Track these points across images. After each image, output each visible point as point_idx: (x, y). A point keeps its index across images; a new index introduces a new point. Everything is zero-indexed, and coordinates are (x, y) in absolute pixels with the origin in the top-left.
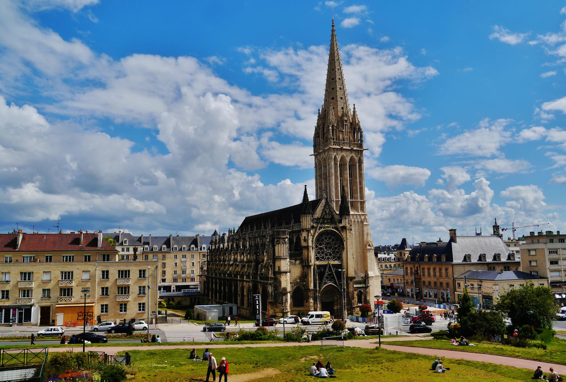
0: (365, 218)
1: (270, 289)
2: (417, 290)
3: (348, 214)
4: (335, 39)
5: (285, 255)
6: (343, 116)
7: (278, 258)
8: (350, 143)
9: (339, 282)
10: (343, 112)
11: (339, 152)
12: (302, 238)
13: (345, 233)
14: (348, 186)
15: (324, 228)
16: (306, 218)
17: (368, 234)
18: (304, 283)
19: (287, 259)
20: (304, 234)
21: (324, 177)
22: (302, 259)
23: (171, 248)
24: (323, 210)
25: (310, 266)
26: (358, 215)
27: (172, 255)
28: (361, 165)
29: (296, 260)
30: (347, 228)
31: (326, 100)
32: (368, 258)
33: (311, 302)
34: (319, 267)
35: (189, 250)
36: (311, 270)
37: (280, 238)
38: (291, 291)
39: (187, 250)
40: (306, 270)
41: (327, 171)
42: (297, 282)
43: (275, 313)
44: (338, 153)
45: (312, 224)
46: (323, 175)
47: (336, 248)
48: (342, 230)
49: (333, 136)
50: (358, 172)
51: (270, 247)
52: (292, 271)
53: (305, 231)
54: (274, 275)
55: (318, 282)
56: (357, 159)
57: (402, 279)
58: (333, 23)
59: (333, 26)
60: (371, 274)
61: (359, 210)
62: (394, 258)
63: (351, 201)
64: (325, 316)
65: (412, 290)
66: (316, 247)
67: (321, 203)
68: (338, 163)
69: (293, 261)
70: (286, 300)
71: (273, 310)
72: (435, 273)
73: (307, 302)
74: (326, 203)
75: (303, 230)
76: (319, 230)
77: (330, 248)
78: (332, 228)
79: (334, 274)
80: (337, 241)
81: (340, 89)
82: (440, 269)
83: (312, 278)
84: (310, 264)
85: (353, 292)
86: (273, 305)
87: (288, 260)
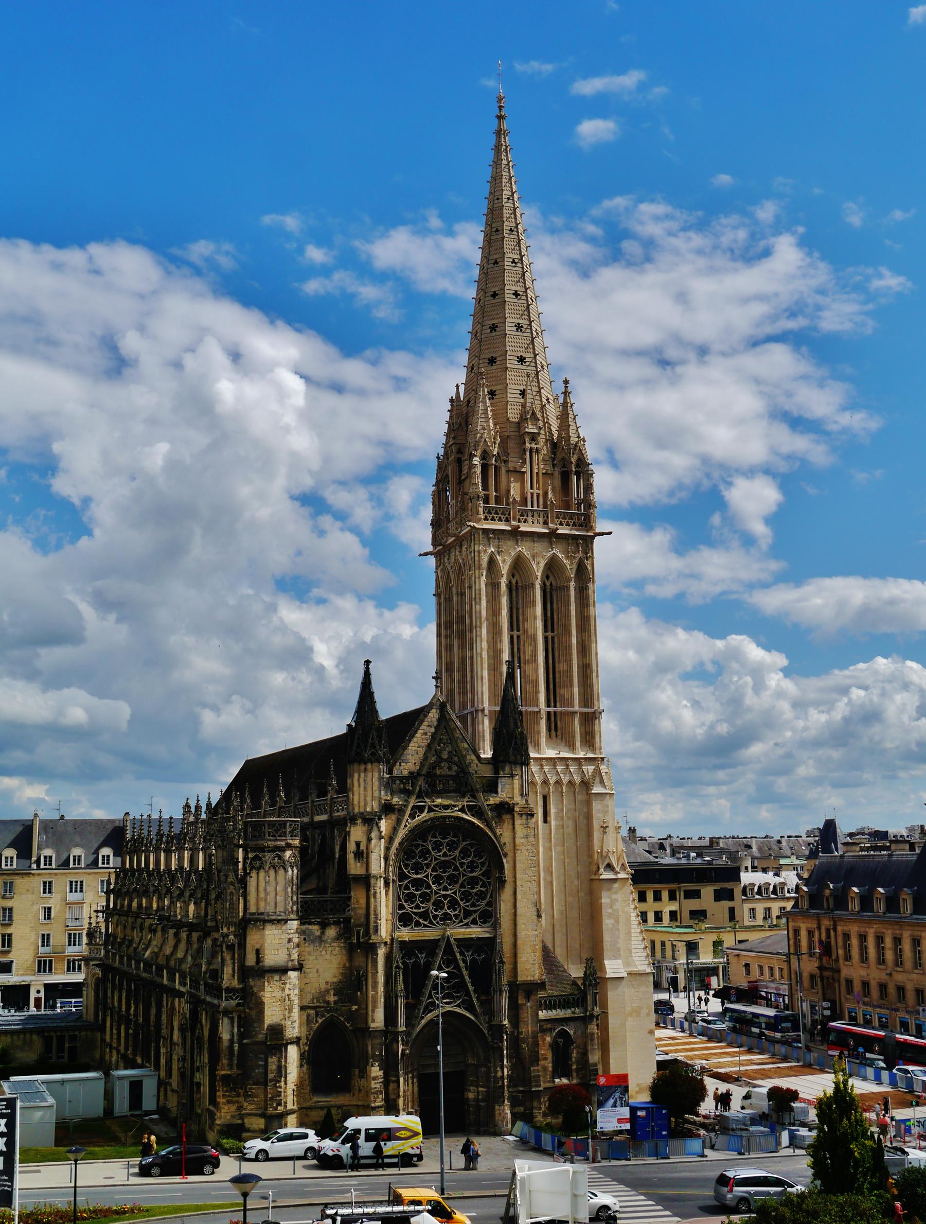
0: (598, 772)
2: (825, 1009)
3: (525, 761)
4: (505, 162)
5: (280, 908)
6: (523, 419)
7: (257, 920)
8: (546, 513)
9: (482, 1003)
10: (524, 406)
11: (508, 545)
12: (351, 847)
13: (507, 826)
14: (536, 661)
15: (430, 810)
16: (362, 775)
17: (604, 828)
18: (354, 1008)
19: (286, 921)
20: (357, 833)
21: (458, 631)
22: (347, 921)
23: (34, 859)
24: (429, 746)
25: (372, 949)
26: (570, 762)
27: (36, 883)
28: (587, 588)
29: (324, 926)
30: (517, 809)
31: (472, 368)
32: (606, 911)
33: (373, 1075)
34: (408, 948)
35: (94, 864)
36: (375, 962)
37: (262, 849)
38: (303, 1035)
39: (88, 866)
40: (359, 960)
41: (467, 607)
42: (328, 1002)
43: (242, 1117)
44: (504, 548)
45: (385, 796)
46: (458, 623)
47: (473, 882)
48: (499, 817)
49: (485, 486)
50: (573, 613)
51: (229, 880)
52: (308, 965)
53: (359, 821)
54: (240, 981)
55: (401, 1002)
56: (570, 566)
57: (785, 966)
58: (500, 108)
59: (500, 118)
60: (613, 967)
61: (578, 744)
62: (797, 886)
63: (549, 713)
64: (402, 1134)
65: (813, 1007)
66: (402, 876)
67: (426, 723)
68: (504, 581)
69: (315, 929)
70: (281, 1071)
71: (233, 1108)
72: (881, 951)
73: (361, 1077)
74: (439, 720)
75: (353, 819)
76: (412, 816)
77: (453, 880)
78: (462, 810)
80: (478, 855)
81: (519, 327)
82: (897, 940)
83: (381, 988)
84: (374, 939)
85: (535, 1037)
86: (233, 1089)
87: (294, 924)
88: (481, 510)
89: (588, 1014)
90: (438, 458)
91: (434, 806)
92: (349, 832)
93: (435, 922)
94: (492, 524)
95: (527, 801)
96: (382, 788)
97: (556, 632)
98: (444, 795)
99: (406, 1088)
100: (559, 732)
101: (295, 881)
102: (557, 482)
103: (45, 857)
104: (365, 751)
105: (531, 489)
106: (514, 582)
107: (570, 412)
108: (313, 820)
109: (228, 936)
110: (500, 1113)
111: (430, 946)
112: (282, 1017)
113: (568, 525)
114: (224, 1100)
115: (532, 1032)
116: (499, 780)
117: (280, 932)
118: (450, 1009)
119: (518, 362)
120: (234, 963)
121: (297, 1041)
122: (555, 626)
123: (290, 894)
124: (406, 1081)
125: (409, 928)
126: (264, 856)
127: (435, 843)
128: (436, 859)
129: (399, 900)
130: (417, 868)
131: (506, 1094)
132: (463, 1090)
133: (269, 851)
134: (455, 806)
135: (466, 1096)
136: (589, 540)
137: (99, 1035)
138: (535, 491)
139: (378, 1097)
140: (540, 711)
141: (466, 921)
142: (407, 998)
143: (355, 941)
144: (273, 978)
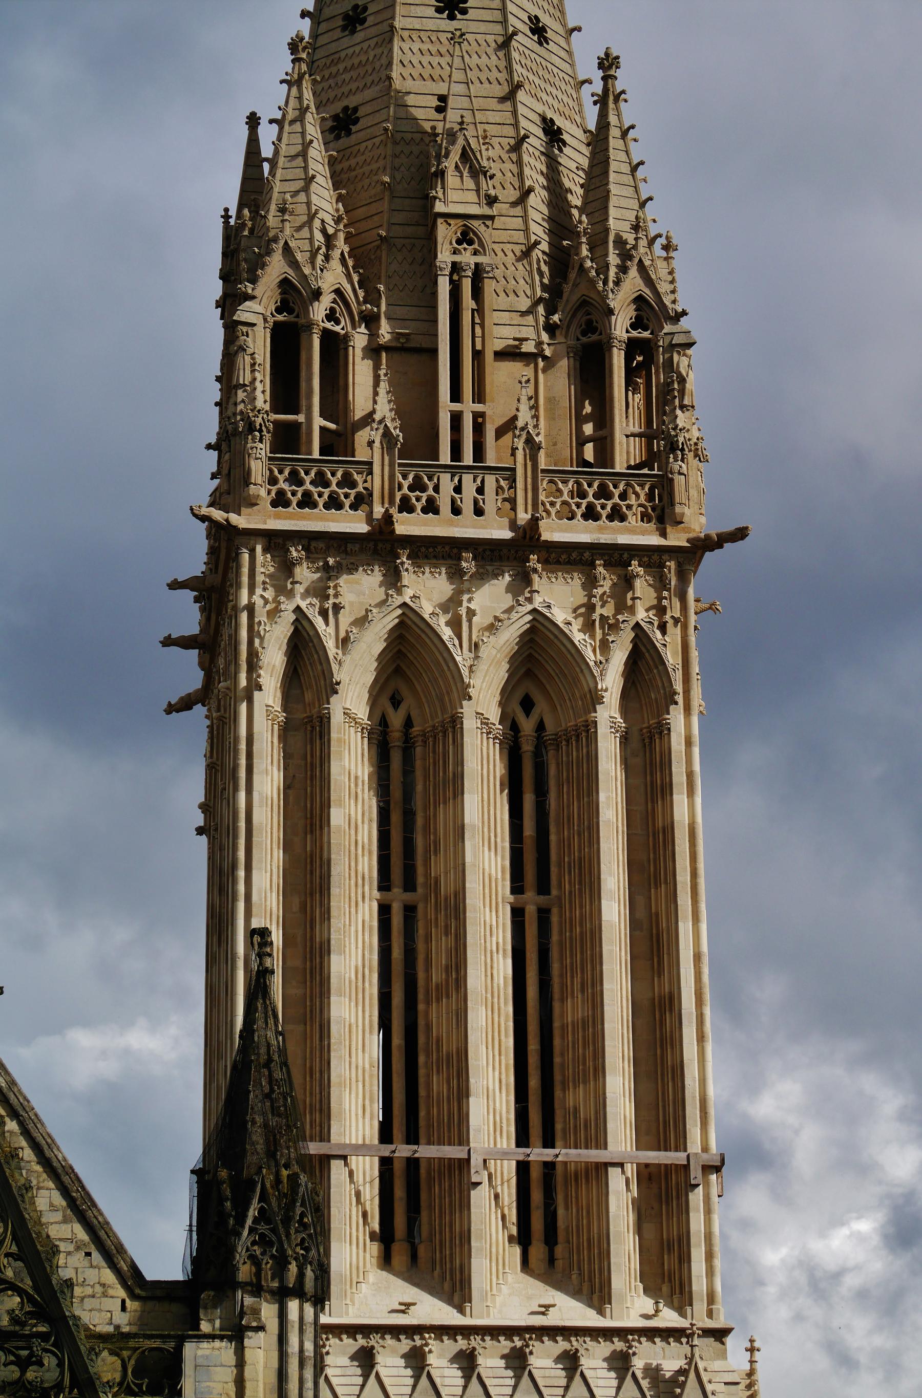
94: (303, 518)
97: (554, 892)
100: (559, 1250)
105: (456, 396)
106: (396, 720)
113: (591, 514)
116: (189, 1349)
119: (439, 10)
122: (554, 870)
138: (468, 407)
140: (468, 1160)
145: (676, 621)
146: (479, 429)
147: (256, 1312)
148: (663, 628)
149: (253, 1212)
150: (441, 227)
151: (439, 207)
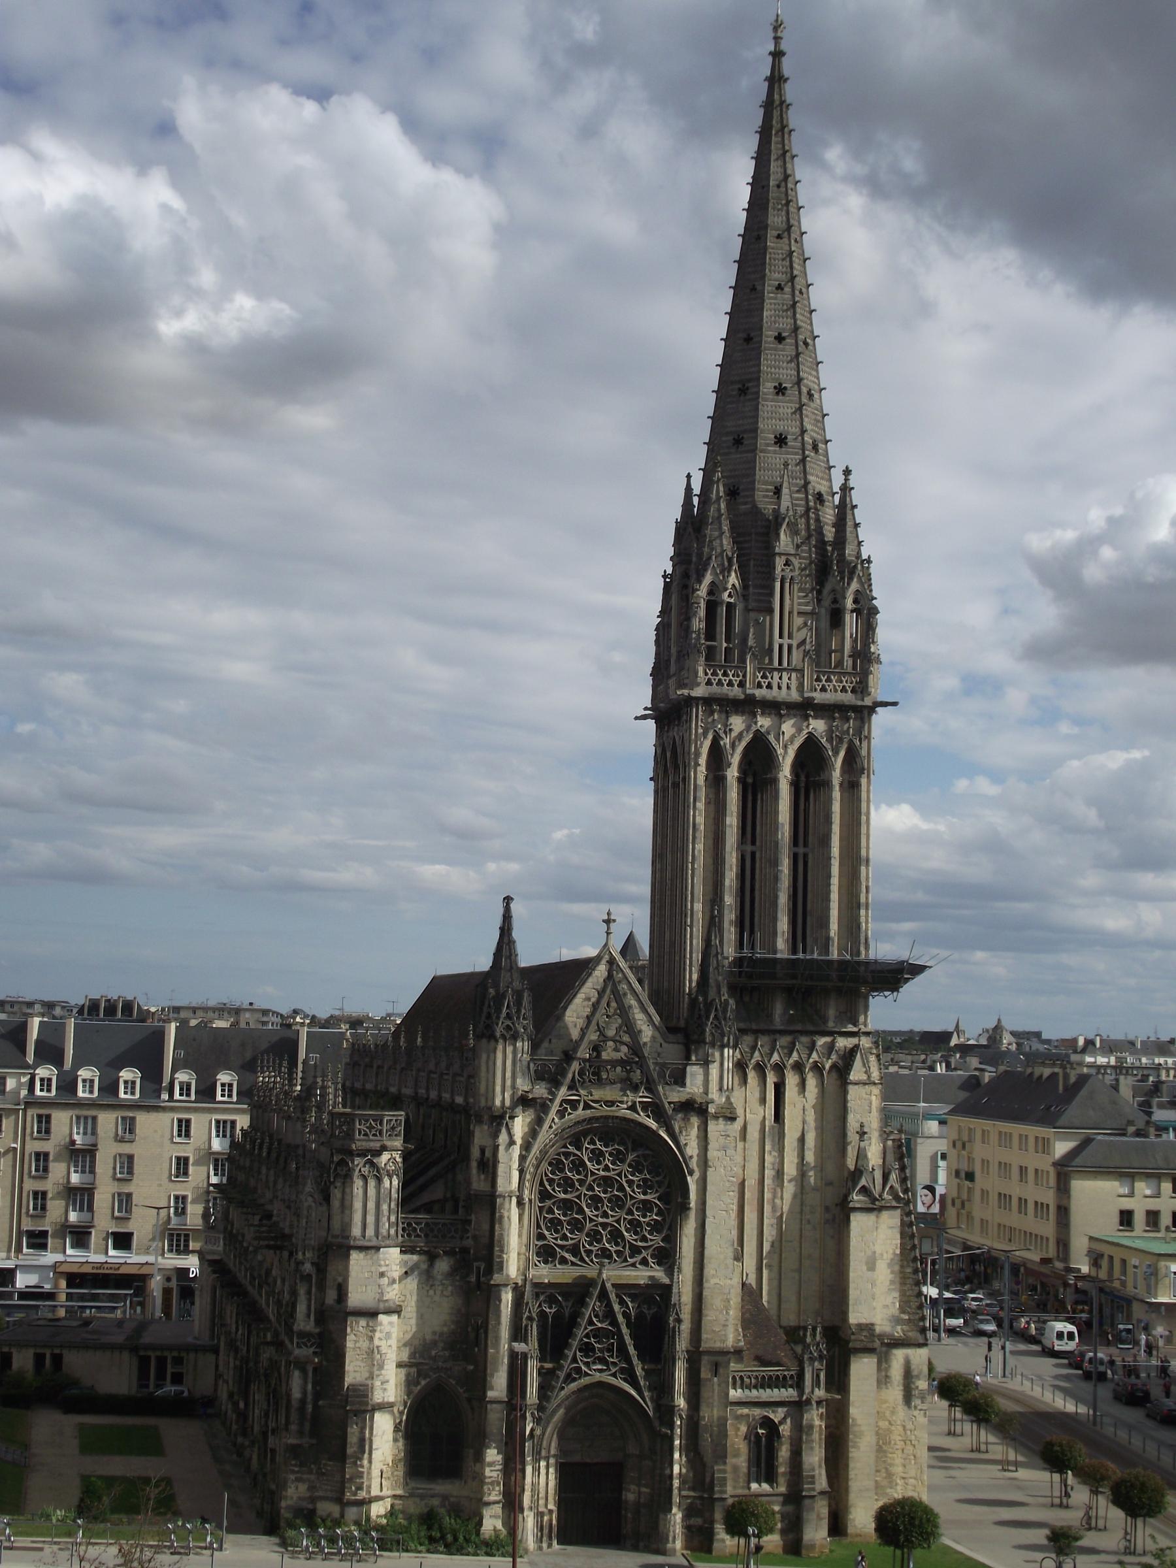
1: (296, 1386)
5: (370, 1232)
12: (475, 1153)
15: (587, 1106)
18: (471, 1367)
19: (377, 1248)
24: (589, 1019)
29: (432, 1258)
37: (351, 1153)
43: (313, 1500)
45: (523, 1085)
51: (309, 1188)
66: (544, 1195)
70: (364, 1445)
71: (303, 1488)
77: (618, 1203)
78: (632, 1108)
79: (625, 1330)
84: (497, 1278)
88: (701, 670)
89: (804, 1398)
90: (665, 576)
91: (592, 1101)
92: (474, 1131)
93: (587, 1259)
95: (728, 1098)
96: (519, 1074)
97: (810, 845)
98: (608, 1088)
99: (535, 1480)
101: (394, 1195)
102: (825, 622)
103: (181, 1084)
104: (497, 1024)
105: (781, 636)
107: (849, 517)
108: (453, 1100)
109: (303, 1264)
110: (665, 1525)
111: (579, 1291)
112: (367, 1375)
114: (292, 1477)
115: (719, 1418)
116: (688, 1068)
117: (370, 1262)
118: (602, 1379)
120: (309, 1300)
121: (384, 1407)
123: (386, 1213)
124: (537, 1470)
125: (549, 1265)
126: (353, 1162)
127: (593, 1151)
128: (593, 1174)
129: (539, 1226)
130: (568, 1184)
131: (676, 1499)
132: (620, 1490)
133: (359, 1155)
134: (620, 1102)
135: (624, 1497)
136: (866, 713)
137: (211, 1357)
138: (786, 642)
139: (493, 1490)
141: (631, 1261)
142: (542, 1359)
143: (473, 1279)
144: (358, 1323)
145: (866, 737)
146: (790, 647)
147: (713, 1055)
148: (860, 741)
149: (712, 1016)
150: (777, 559)
151: (777, 550)
